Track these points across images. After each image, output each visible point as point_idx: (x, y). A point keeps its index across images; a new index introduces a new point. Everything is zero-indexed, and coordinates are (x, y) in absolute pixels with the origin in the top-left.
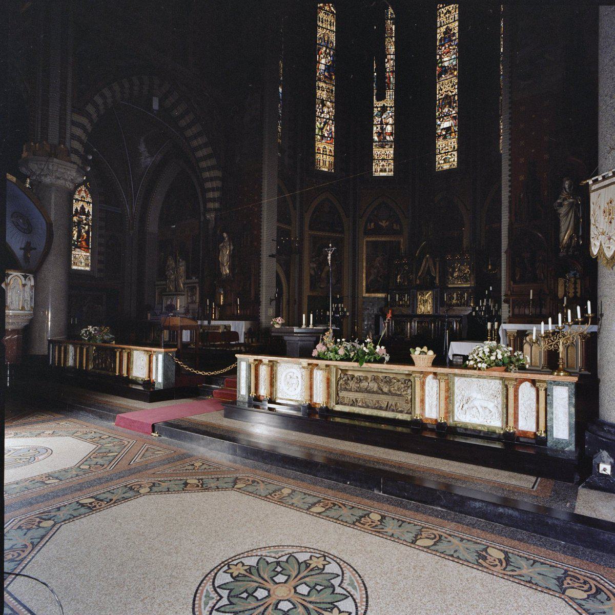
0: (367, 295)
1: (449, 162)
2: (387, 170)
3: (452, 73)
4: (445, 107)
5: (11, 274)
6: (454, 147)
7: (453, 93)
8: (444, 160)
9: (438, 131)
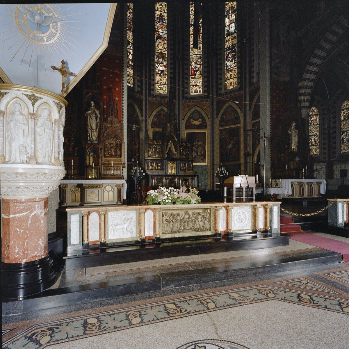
1: (162, 90)
3: (164, 41)
4: (160, 58)
5: (40, 98)
6: (165, 83)
7: (165, 53)
8: (160, 88)
9: (156, 70)
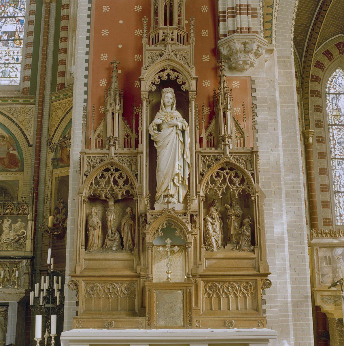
1: (9, 77)
4: (10, 5)
6: (17, 59)
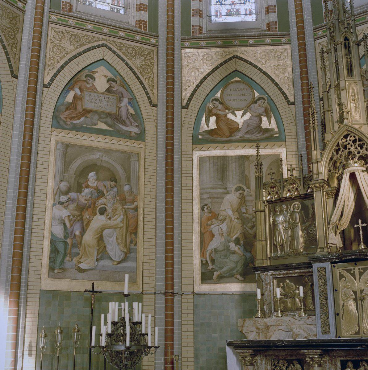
0: (206, 288)
2: (243, 12)
